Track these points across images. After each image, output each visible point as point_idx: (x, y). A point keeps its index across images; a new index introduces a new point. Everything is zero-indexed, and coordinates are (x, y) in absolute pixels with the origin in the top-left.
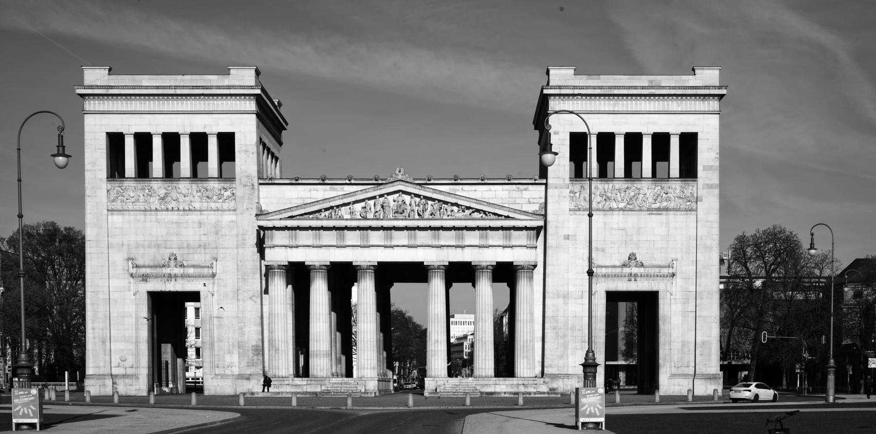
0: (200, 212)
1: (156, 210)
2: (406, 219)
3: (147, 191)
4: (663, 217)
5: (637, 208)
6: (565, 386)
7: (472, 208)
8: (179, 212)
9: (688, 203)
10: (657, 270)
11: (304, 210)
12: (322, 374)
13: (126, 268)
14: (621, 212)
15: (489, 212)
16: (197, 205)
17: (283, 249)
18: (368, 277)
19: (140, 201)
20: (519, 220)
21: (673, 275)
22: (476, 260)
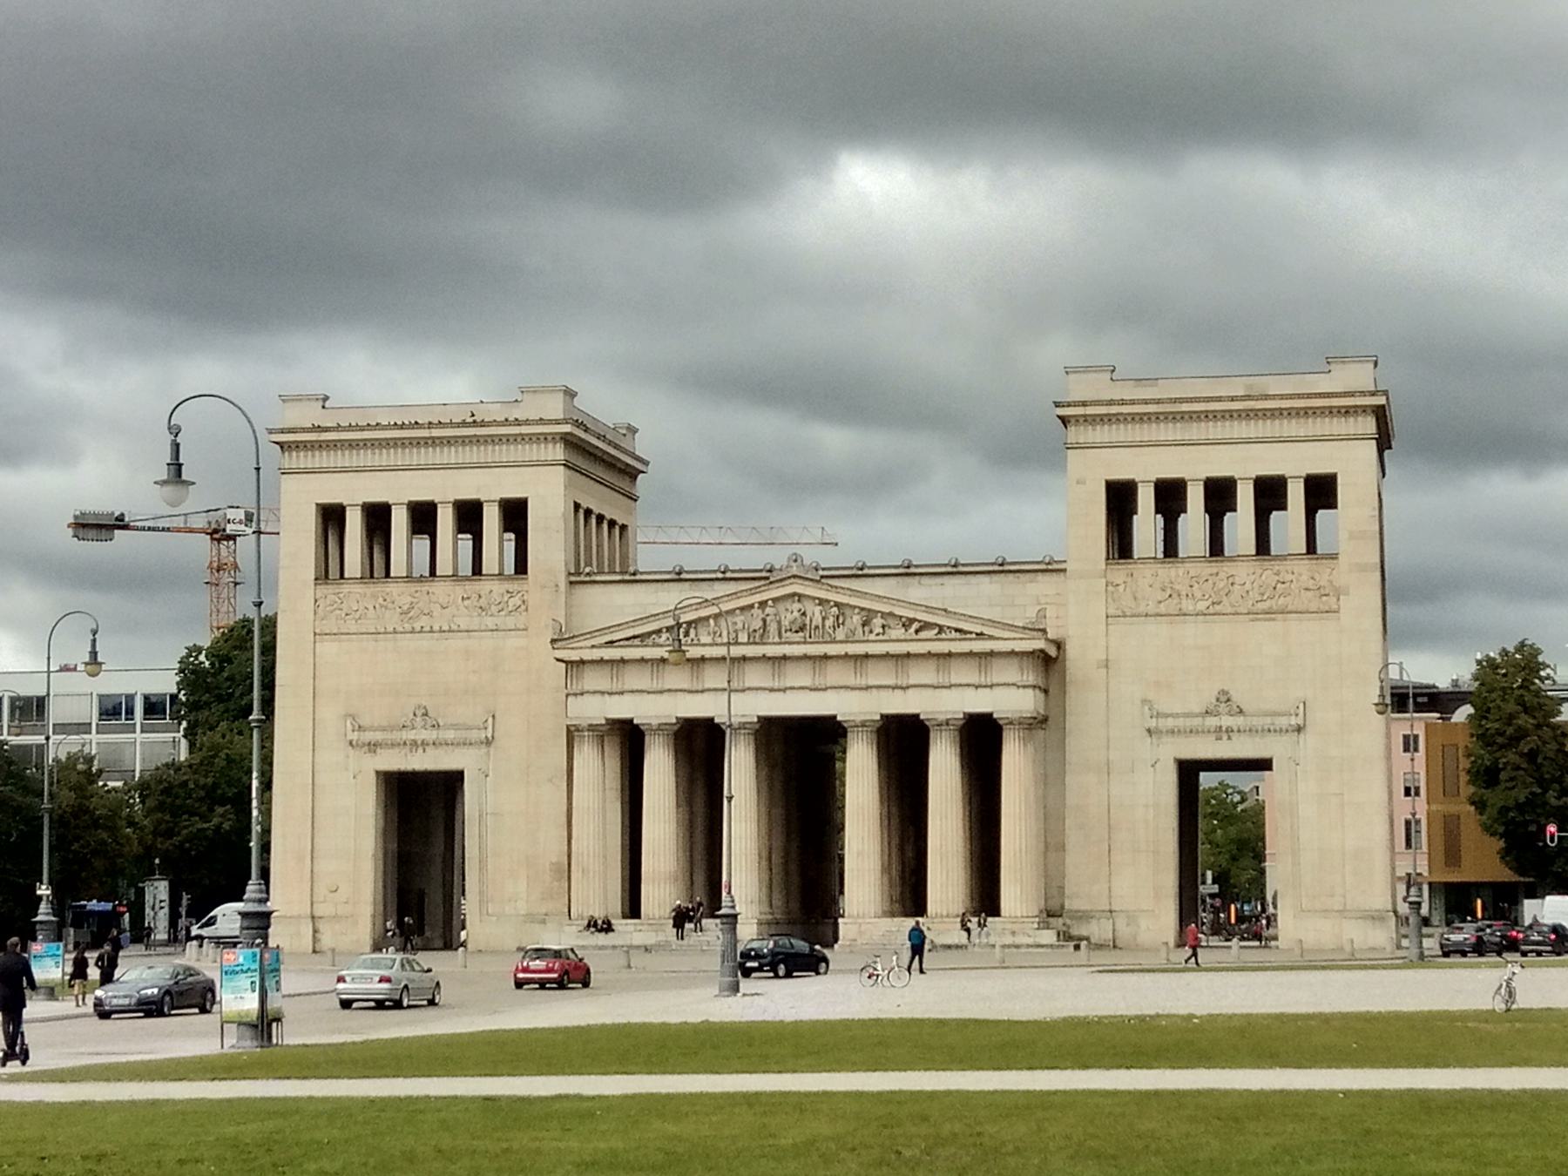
2: (805, 643)
3: (381, 600)
4: (1277, 626)
5: (1230, 610)
7: (920, 621)
9: (1324, 598)
10: (1268, 720)
11: (631, 629)
12: (662, 913)
14: (1201, 618)
15: (949, 627)
17: (598, 697)
18: (742, 743)
19: (369, 616)
20: (1006, 639)
21: (1299, 729)
22: (929, 710)
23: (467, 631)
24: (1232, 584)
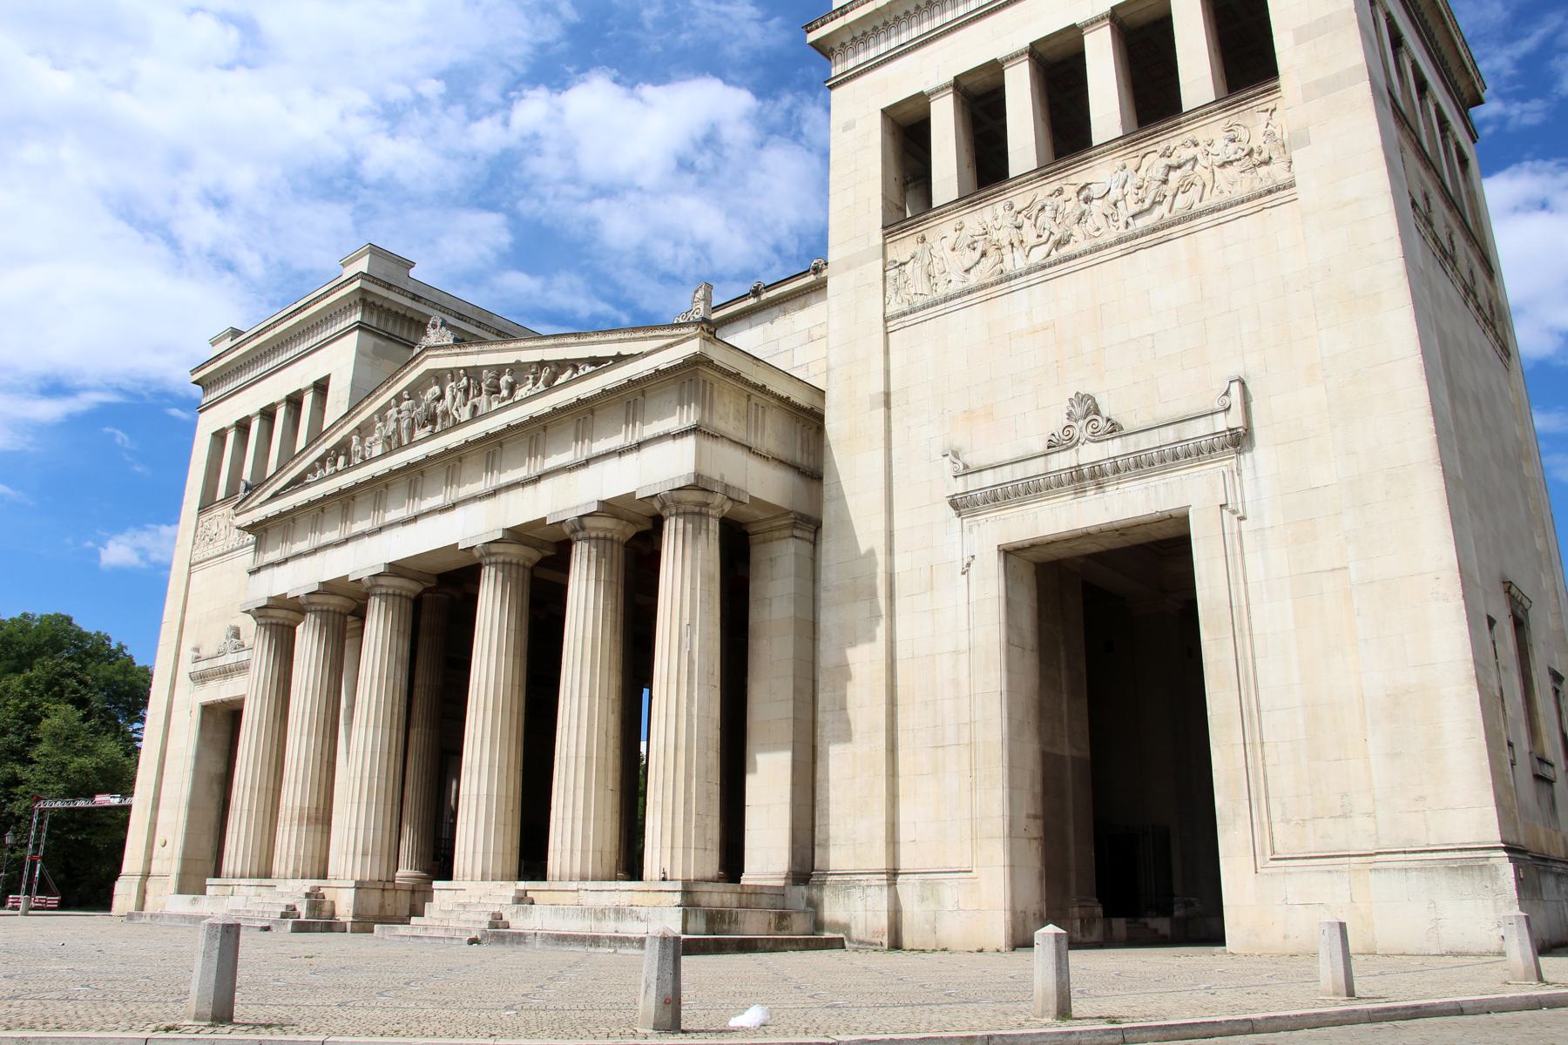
4: (1179, 249)
5: (1085, 245)
6: (870, 914)
9: (1263, 170)
21: (1240, 440)
24: (1088, 200)
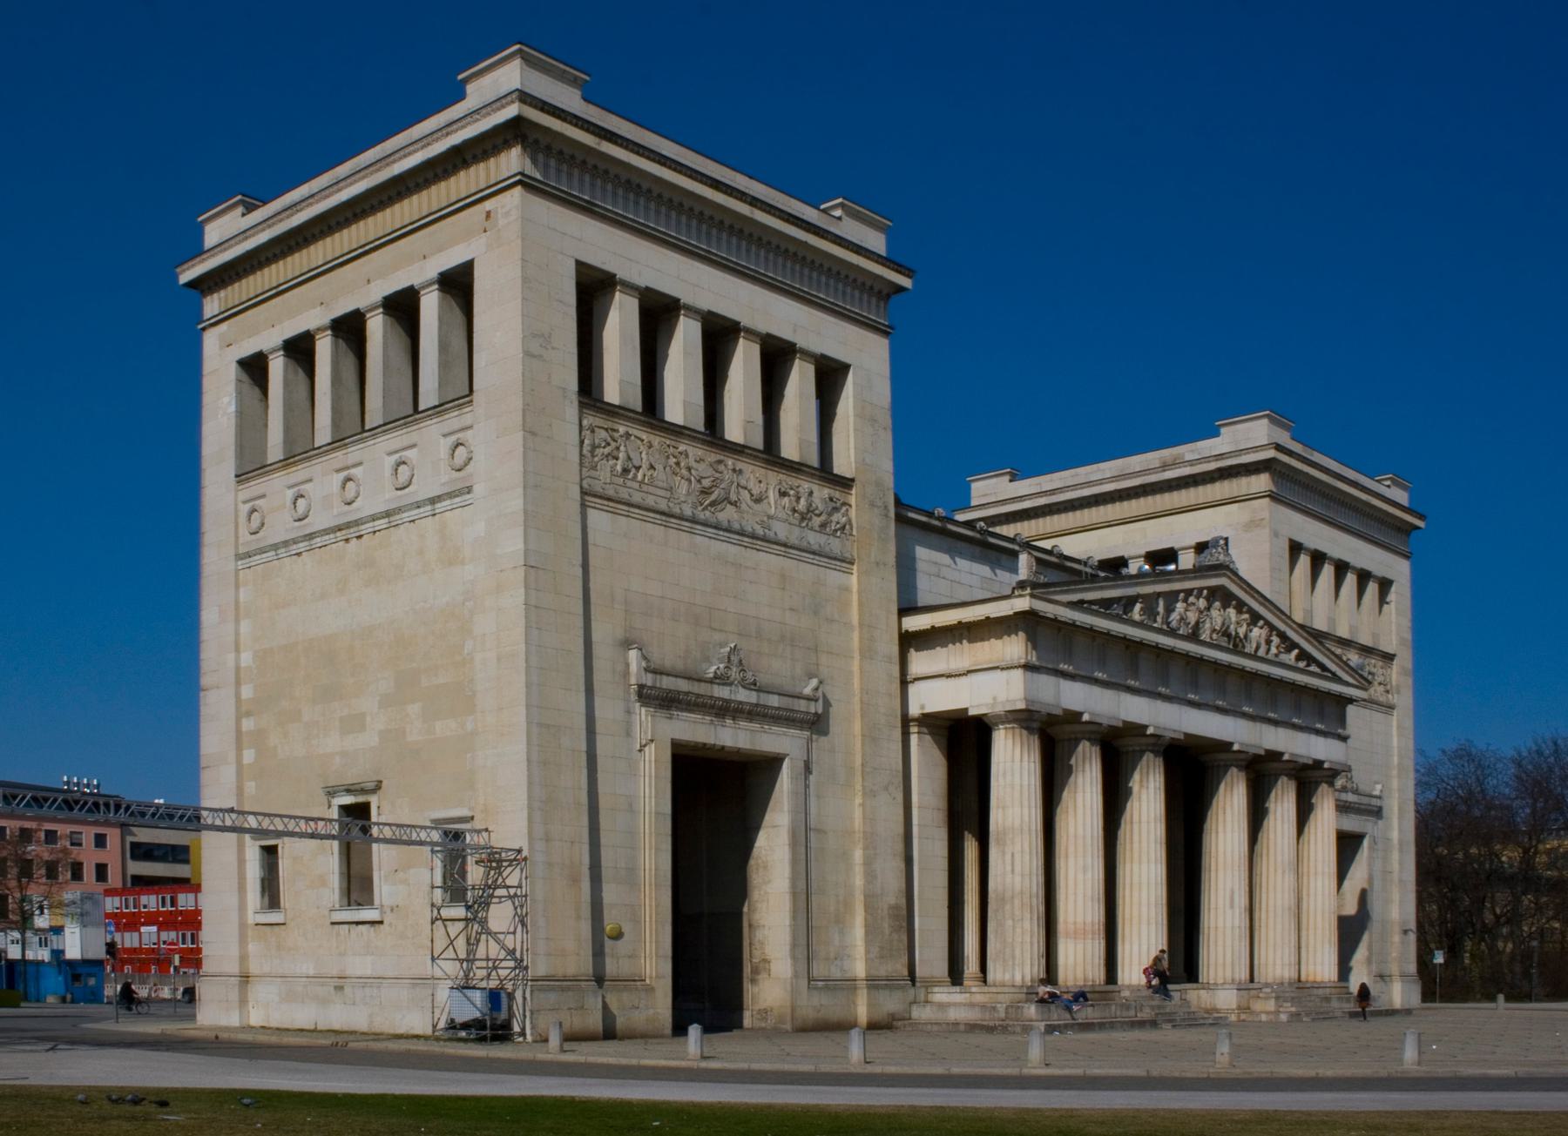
0: (783, 549)
1: (694, 521)
8: (740, 538)
13: (620, 667)
16: (781, 530)
23: (785, 545)
